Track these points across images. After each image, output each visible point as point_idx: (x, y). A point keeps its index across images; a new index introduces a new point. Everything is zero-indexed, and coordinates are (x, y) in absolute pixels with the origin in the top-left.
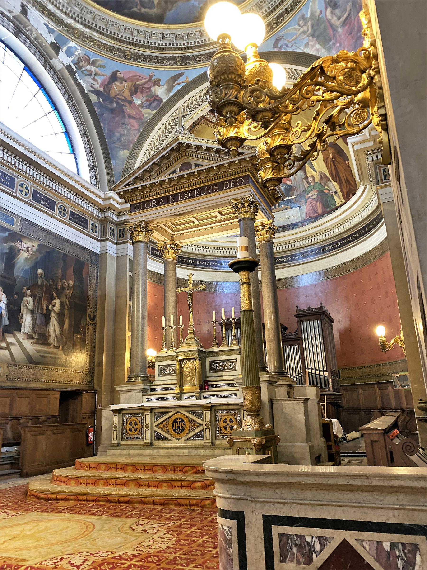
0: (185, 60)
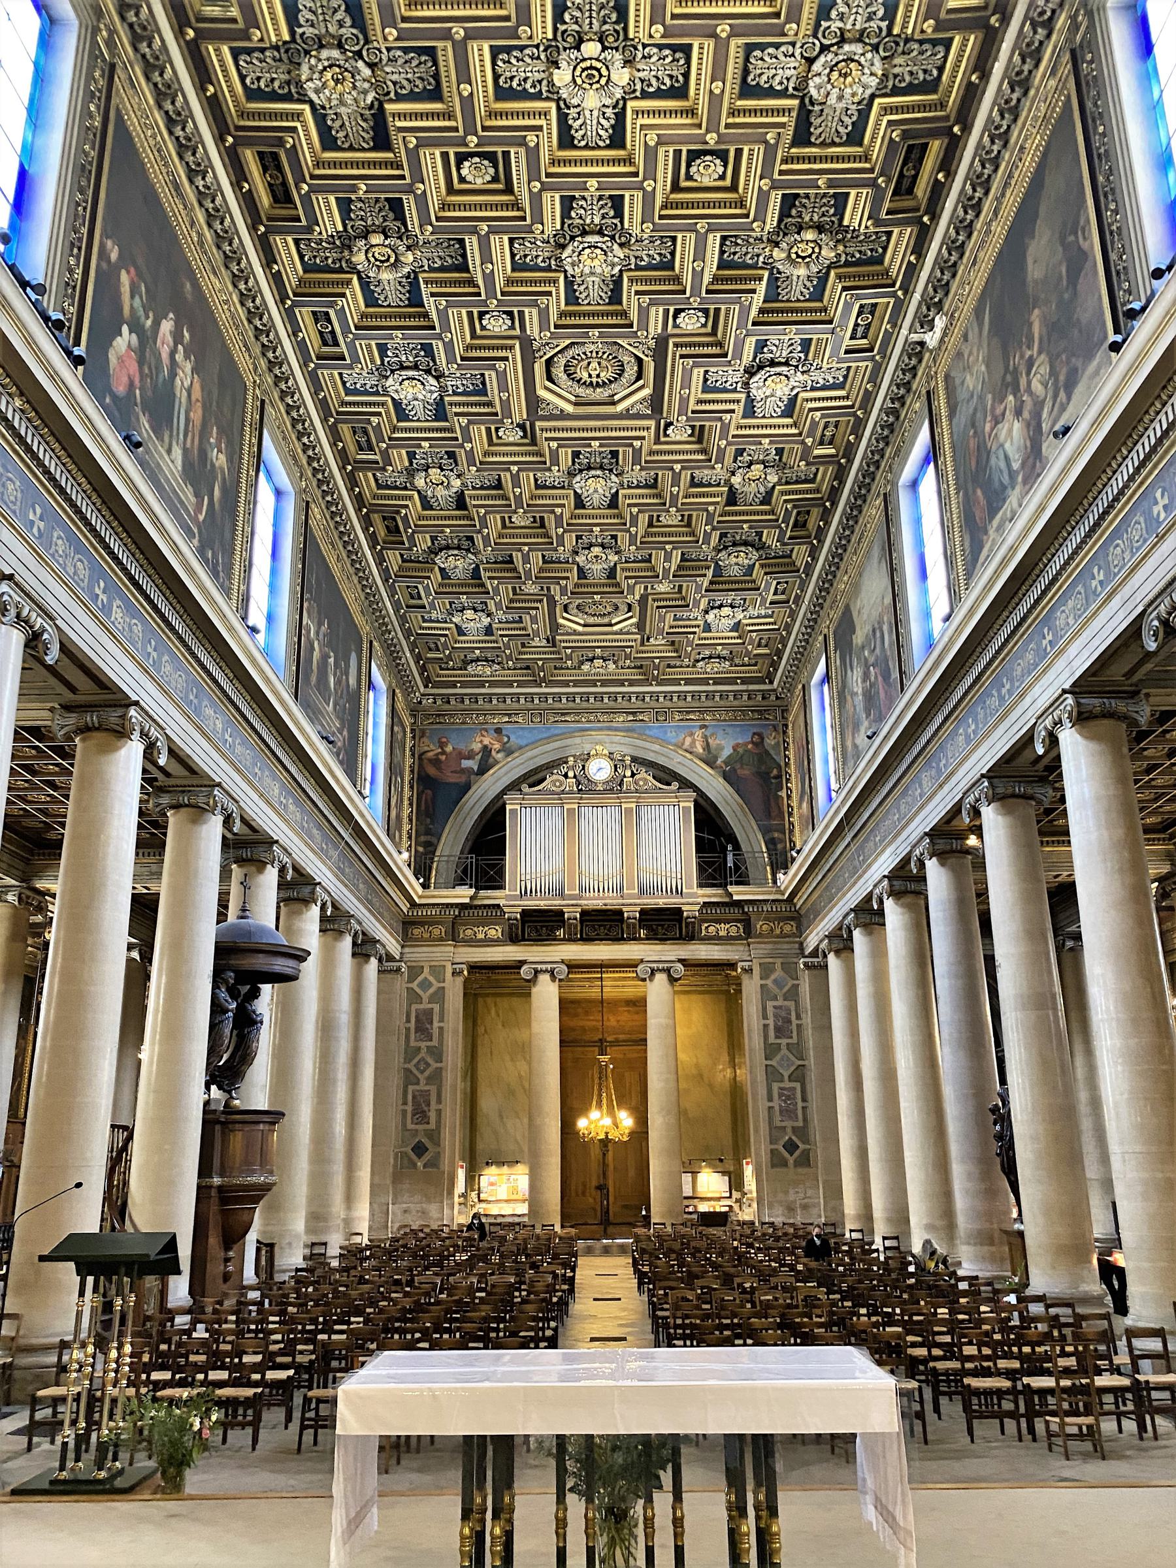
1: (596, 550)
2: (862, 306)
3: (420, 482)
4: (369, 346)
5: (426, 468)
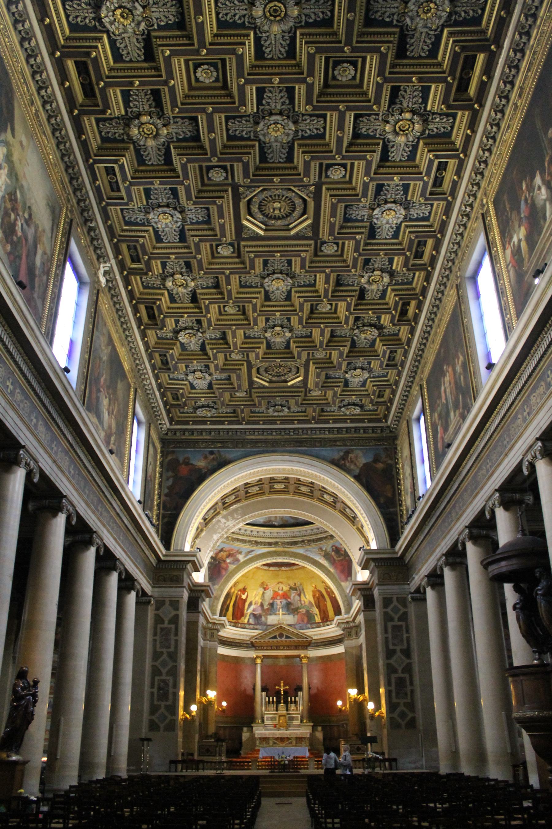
0: (257, 543)
1: (278, 329)
2: (440, 162)
3: (169, 284)
4: (138, 190)
5: (172, 275)
